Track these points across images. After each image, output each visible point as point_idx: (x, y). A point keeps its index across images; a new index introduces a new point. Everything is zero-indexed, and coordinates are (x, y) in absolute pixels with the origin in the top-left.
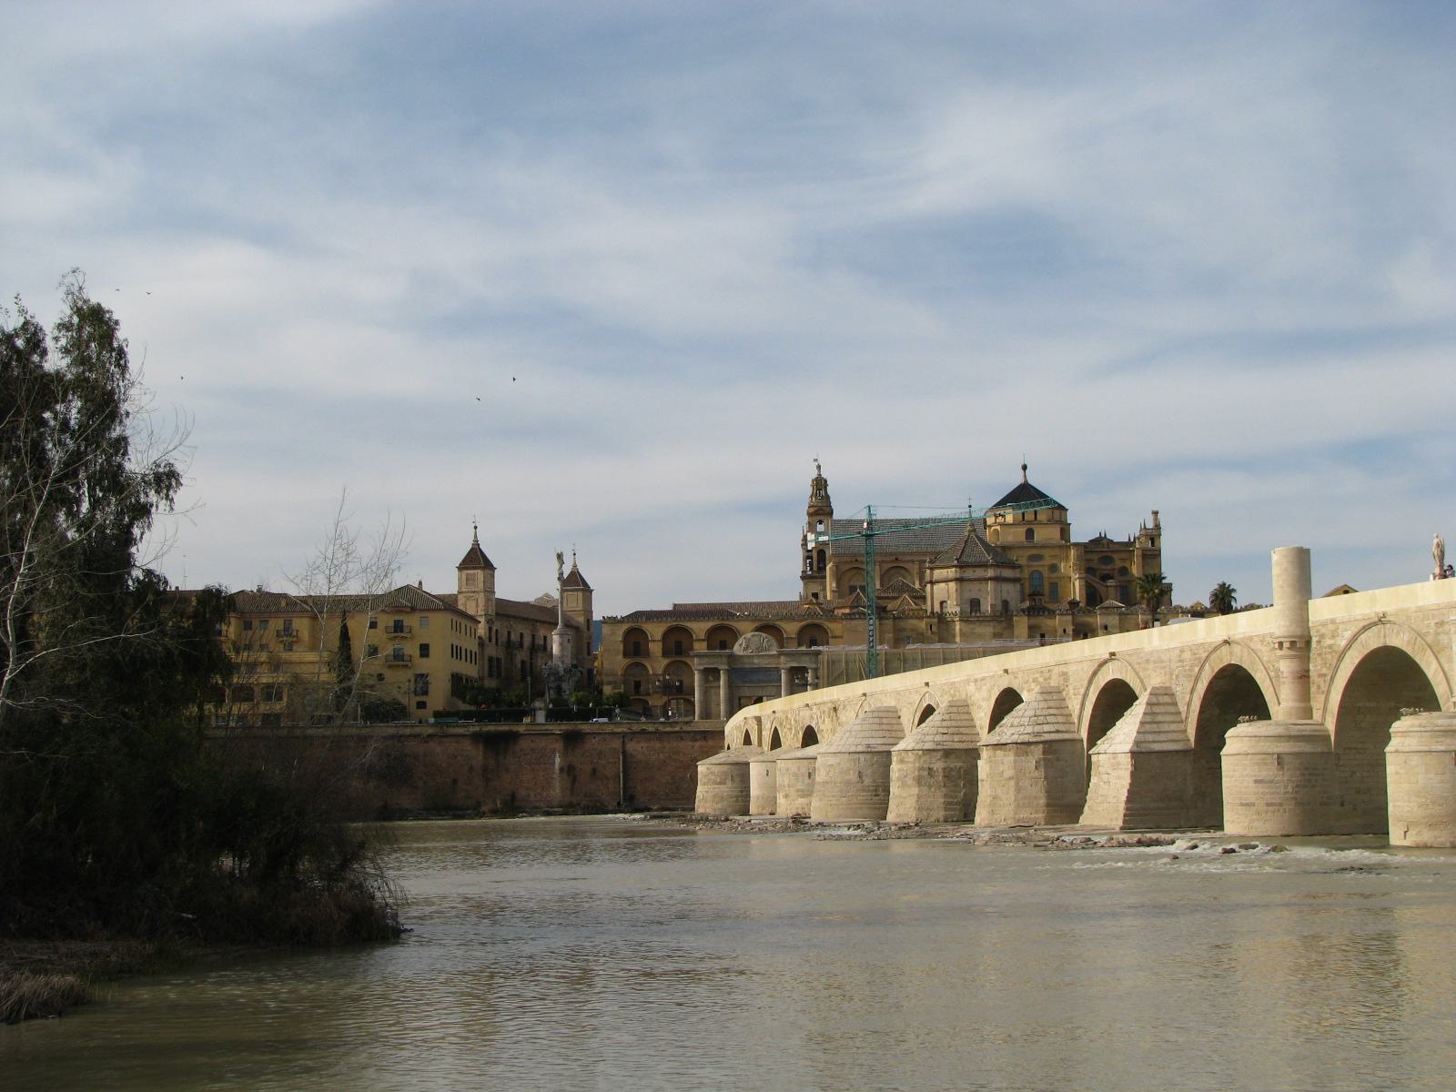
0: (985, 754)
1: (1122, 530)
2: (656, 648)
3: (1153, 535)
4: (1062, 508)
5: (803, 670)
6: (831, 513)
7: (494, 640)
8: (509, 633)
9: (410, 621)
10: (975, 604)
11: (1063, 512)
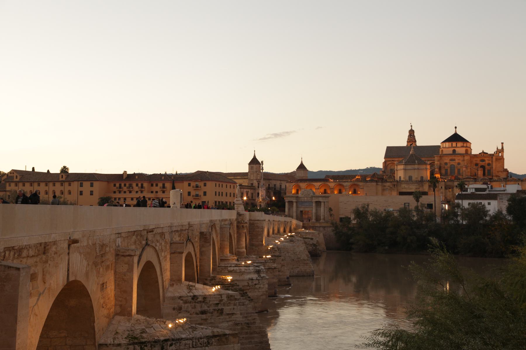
1: (491, 150)
3: (502, 150)
4: (466, 141)
5: (320, 202)
6: (415, 141)
8: (269, 185)
9: (201, 184)
10: (410, 178)
11: (468, 143)
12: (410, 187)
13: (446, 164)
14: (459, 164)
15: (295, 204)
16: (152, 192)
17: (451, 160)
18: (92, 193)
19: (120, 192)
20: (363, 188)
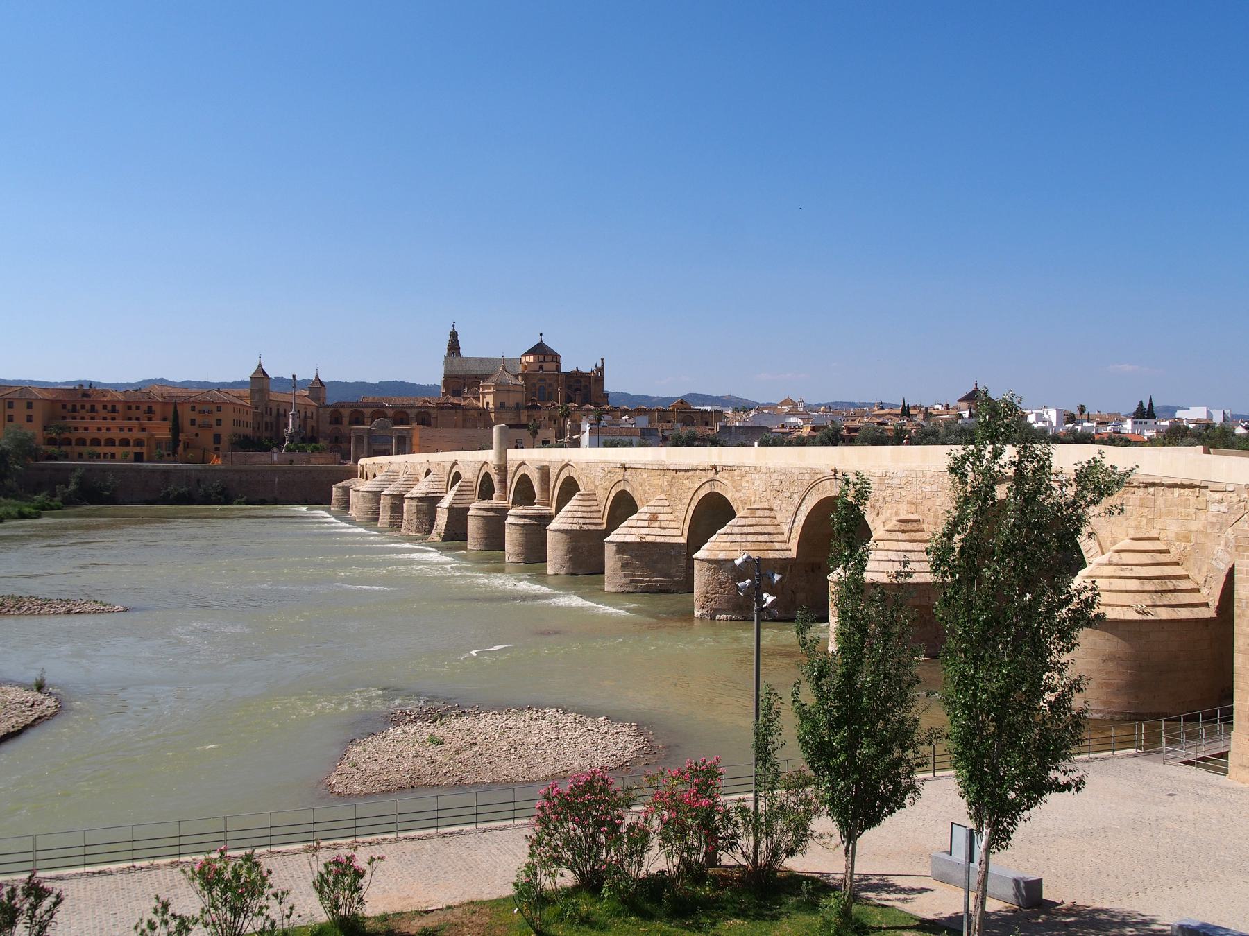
0: (406, 501)
1: (586, 369)
2: (346, 421)
7: (269, 413)
12: (503, 417)
13: (534, 385)
14: (550, 385)
15: (365, 440)
16: (130, 419)
17: (540, 380)
18: (29, 419)
19: (74, 418)
20: (437, 418)
